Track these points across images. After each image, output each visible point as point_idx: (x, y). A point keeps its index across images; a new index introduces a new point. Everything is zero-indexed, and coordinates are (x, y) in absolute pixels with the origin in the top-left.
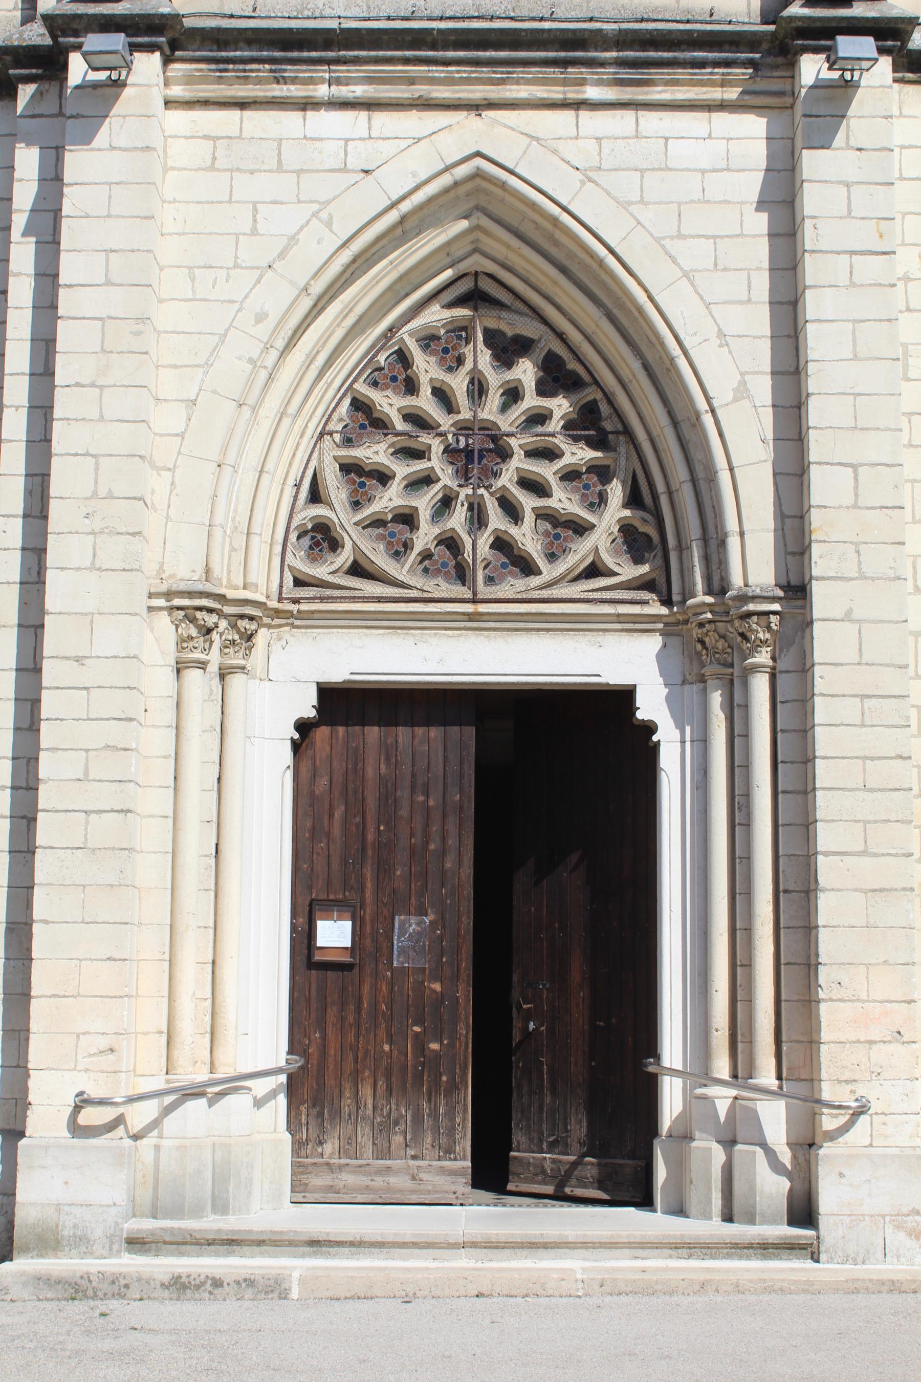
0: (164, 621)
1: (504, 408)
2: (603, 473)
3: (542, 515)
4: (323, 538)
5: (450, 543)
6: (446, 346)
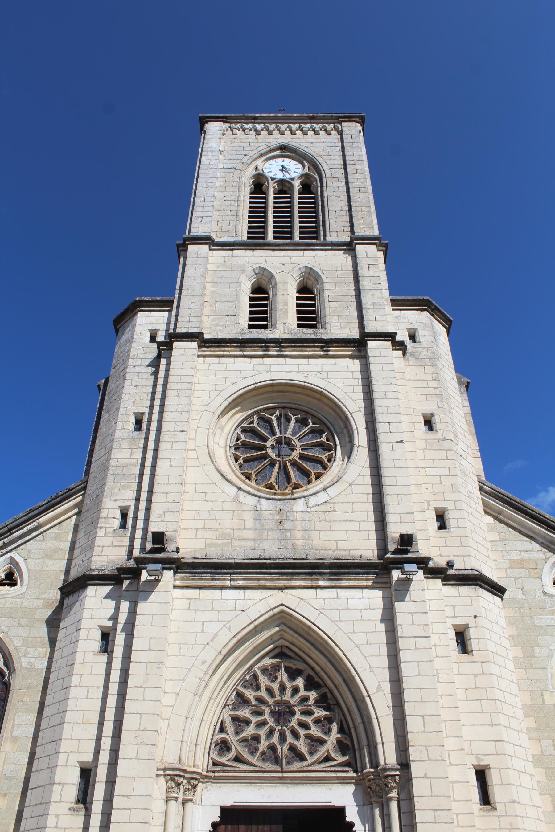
0: (162, 780)
1: (292, 696)
2: (329, 720)
3: (307, 737)
4: (224, 746)
5: (272, 748)
6: (271, 673)
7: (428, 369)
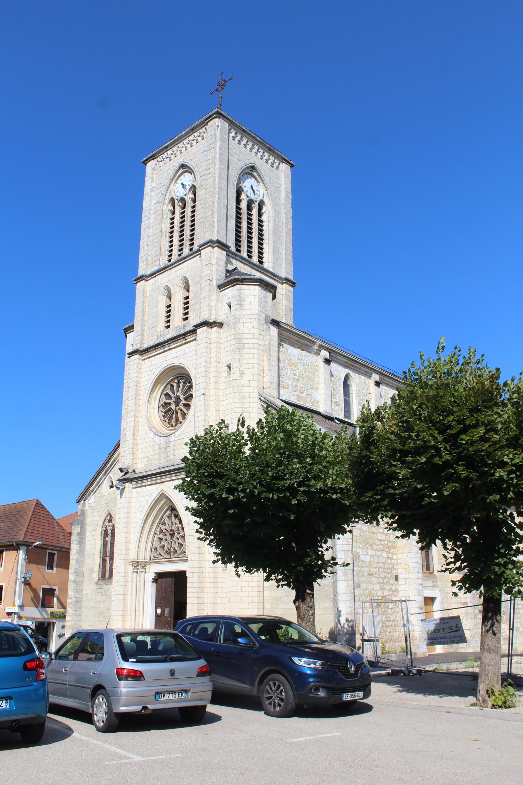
7: (232, 332)
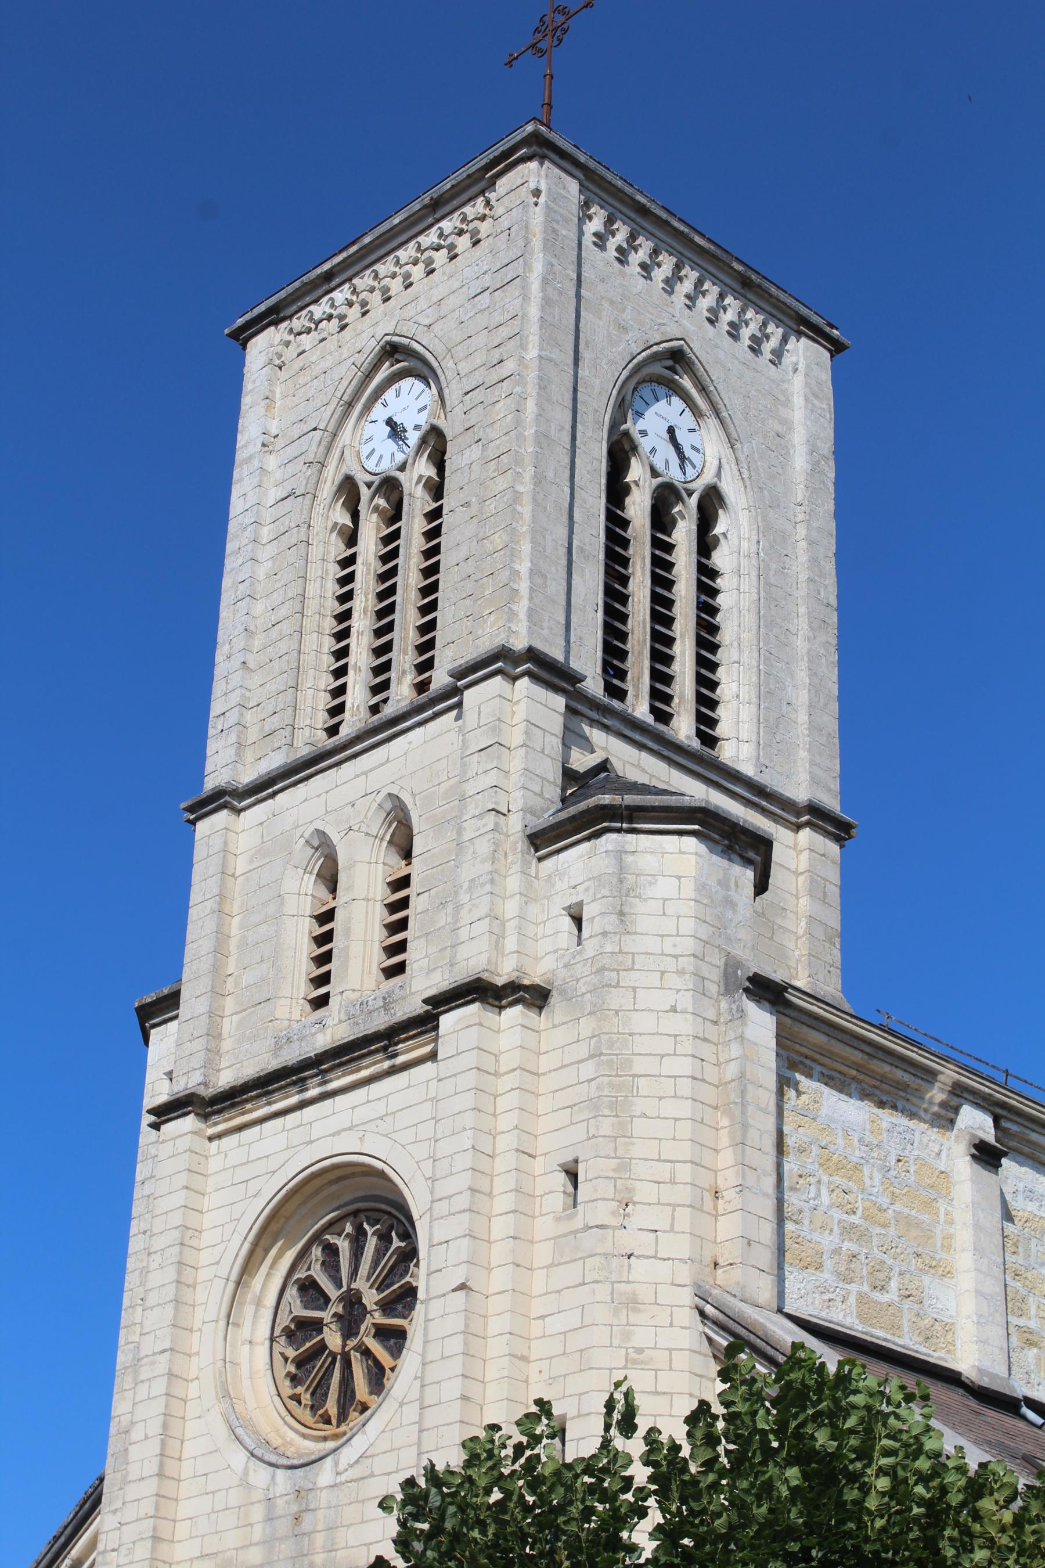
7: (587, 1026)
